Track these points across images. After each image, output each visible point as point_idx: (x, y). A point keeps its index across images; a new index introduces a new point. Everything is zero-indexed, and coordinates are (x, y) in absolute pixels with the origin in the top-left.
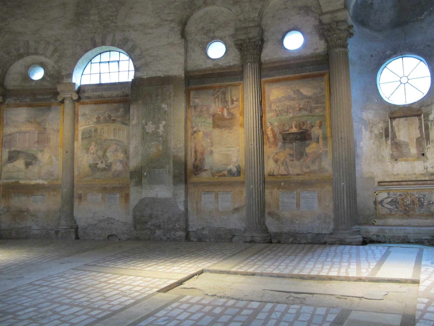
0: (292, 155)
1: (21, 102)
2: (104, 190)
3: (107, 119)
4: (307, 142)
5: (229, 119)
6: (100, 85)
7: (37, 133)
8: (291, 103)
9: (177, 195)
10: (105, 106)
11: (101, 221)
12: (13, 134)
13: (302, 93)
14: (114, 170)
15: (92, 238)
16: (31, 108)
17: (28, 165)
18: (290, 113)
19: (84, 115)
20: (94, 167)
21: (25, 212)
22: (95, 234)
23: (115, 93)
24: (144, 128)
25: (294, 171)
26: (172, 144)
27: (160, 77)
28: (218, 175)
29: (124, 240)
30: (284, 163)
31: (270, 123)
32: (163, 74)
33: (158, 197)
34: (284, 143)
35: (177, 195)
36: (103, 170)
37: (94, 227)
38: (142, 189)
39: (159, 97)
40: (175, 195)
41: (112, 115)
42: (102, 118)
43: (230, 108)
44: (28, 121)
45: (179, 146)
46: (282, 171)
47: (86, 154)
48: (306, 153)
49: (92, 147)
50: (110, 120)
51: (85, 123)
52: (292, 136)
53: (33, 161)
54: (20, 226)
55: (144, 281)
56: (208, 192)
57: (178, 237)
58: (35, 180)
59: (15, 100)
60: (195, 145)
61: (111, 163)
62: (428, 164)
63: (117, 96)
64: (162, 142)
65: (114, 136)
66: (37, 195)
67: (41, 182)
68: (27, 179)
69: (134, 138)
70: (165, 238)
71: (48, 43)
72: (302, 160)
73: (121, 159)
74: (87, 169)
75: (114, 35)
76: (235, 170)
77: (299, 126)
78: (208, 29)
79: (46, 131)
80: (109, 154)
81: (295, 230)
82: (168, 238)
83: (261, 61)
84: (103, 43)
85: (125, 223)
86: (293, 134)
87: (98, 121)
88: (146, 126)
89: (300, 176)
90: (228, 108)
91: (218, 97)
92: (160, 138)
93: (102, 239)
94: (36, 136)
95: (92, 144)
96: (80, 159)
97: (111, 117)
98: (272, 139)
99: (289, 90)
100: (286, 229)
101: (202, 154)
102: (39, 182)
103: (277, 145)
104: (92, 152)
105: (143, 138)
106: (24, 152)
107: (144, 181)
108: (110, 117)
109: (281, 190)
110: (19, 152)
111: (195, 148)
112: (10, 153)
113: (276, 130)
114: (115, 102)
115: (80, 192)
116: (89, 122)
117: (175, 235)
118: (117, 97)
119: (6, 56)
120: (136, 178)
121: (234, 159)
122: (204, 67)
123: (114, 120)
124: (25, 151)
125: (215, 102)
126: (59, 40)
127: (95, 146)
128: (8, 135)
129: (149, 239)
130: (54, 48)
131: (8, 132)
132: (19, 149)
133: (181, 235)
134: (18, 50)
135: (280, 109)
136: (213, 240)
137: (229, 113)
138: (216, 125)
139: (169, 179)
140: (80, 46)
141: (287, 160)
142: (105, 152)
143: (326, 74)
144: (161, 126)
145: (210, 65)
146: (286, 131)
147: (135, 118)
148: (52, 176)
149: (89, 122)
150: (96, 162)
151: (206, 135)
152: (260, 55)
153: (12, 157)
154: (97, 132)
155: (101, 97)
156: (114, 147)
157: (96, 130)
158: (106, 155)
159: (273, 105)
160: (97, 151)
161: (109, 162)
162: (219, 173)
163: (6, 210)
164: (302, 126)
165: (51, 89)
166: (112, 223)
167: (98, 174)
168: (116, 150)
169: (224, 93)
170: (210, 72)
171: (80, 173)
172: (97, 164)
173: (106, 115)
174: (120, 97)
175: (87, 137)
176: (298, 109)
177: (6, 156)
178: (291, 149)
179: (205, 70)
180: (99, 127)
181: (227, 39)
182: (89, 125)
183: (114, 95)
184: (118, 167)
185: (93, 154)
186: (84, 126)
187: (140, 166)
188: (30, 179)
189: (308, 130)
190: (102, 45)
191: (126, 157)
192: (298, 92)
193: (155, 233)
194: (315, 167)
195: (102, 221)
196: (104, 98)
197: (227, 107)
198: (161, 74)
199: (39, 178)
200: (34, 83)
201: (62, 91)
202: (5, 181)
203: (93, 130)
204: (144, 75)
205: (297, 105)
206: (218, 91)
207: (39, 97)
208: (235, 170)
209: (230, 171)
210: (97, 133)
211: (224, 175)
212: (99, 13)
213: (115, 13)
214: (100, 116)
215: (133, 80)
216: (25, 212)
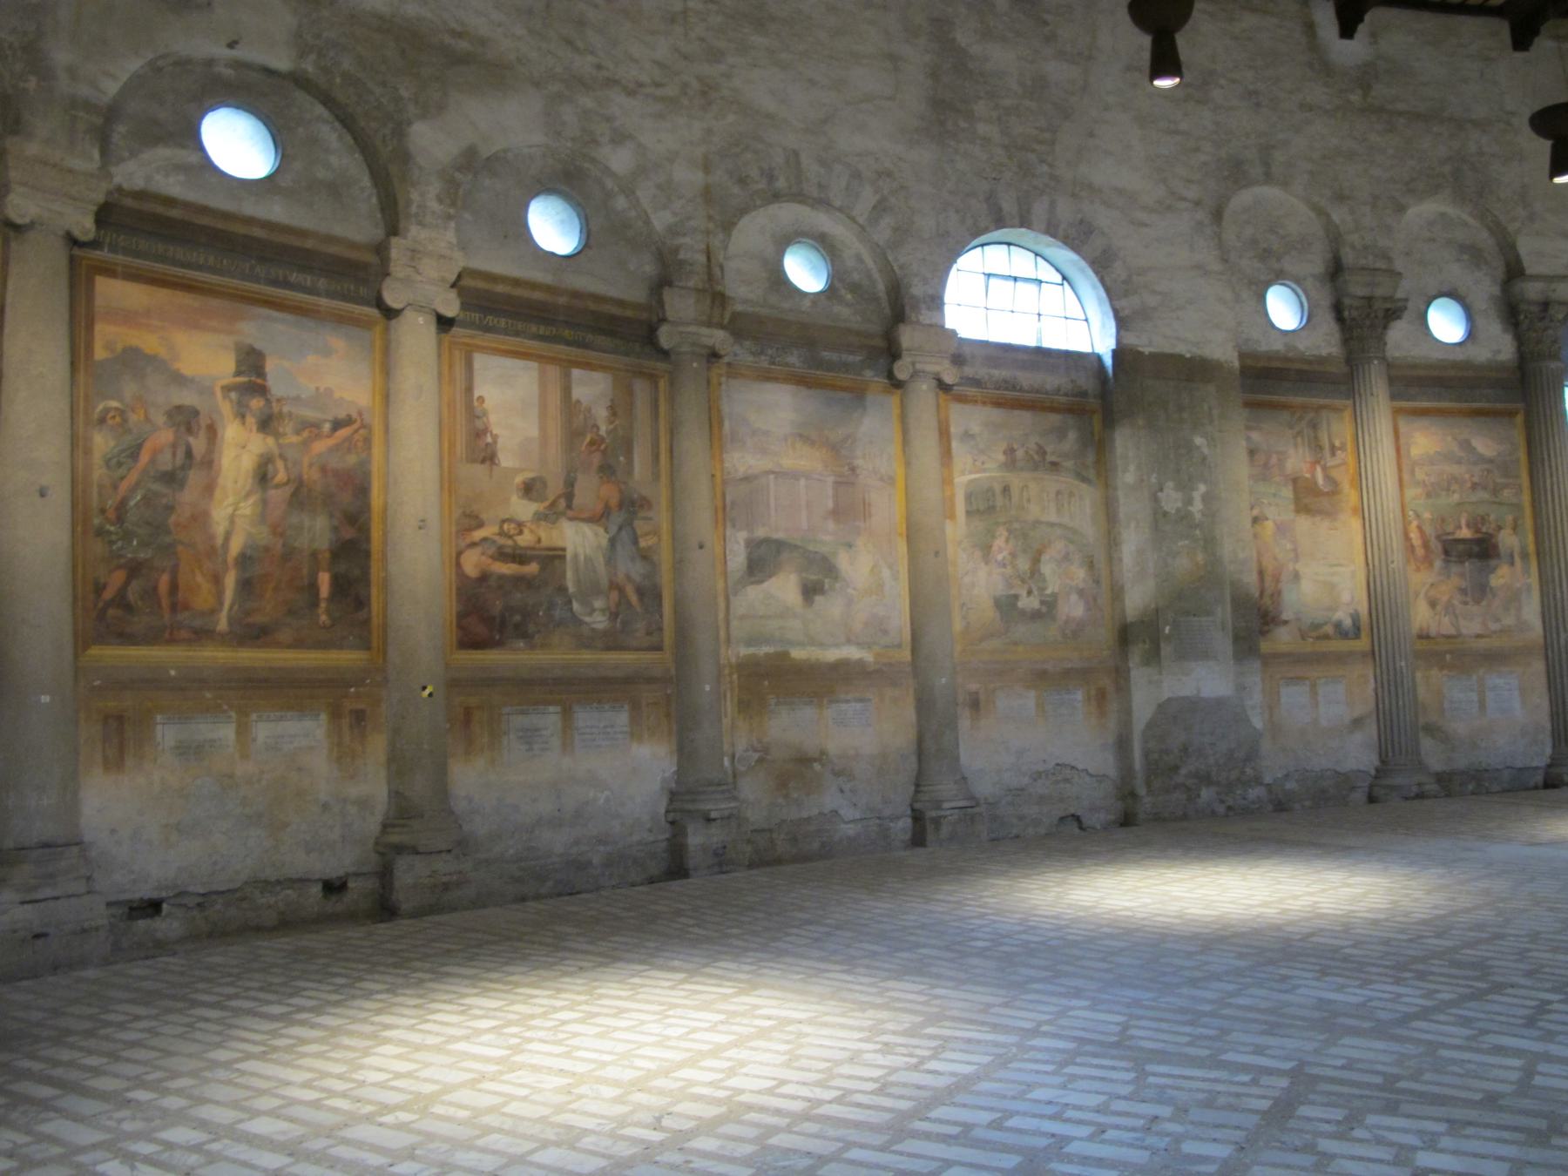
0: (1463, 591)
1: (774, 363)
2: (1041, 678)
3: (1036, 457)
4: (1493, 562)
5: (1327, 493)
6: (1039, 351)
7: (831, 479)
8: (1455, 469)
9: (1245, 688)
10: (1026, 417)
11: (1037, 776)
12: (756, 477)
13: (1475, 449)
14: (1064, 618)
15: (1015, 831)
16: (803, 391)
17: (810, 591)
18: (1454, 492)
19: (967, 436)
20: (1006, 606)
21: (815, 760)
22: (1021, 818)
23: (1052, 381)
24: (1156, 499)
25: (1471, 627)
26: (1227, 549)
27: (1181, 357)
28: (1314, 634)
29: (1099, 827)
30: (1450, 608)
31: (1415, 511)
32: (1189, 352)
33: (1202, 695)
34: (1447, 561)
35: (1245, 688)
36: (1036, 616)
37: (1019, 795)
38: (1160, 673)
39: (1185, 415)
40: (1241, 688)
41: (1049, 449)
42: (1020, 453)
43: (1328, 464)
44: (801, 436)
45: (1241, 556)
46: (1446, 627)
47: (983, 565)
48: (1491, 589)
49: (999, 542)
50: (1042, 463)
51: (974, 464)
52: (1461, 547)
53: (826, 581)
54: (805, 815)
55: (558, 1023)
56: (1297, 680)
57: (1253, 803)
58: (837, 645)
59: (753, 354)
60: (1259, 554)
61: (1055, 596)
63: (1057, 391)
64: (1202, 543)
65: (1059, 511)
66: (847, 701)
67: (853, 653)
68: (813, 642)
69: (1133, 525)
70: (1221, 809)
71: (857, 175)
72: (1484, 603)
73: (1081, 585)
74: (989, 613)
75: (1053, 204)
76: (1348, 622)
77: (1474, 524)
78: (1265, 246)
79: (857, 476)
80: (1047, 569)
81: (1480, 763)
82: (1229, 808)
83: (580, 248)
84: (1024, 222)
85: (1100, 778)
86: (1463, 541)
87: (1011, 463)
88: (1159, 494)
89: (1484, 640)
90: (1325, 465)
91: (1299, 433)
92: (1198, 532)
93: (1042, 831)
94: (830, 492)
95: (998, 533)
96: (967, 580)
97: (1045, 453)
99: (1449, 438)
100: (1461, 762)
101: (1277, 580)
102: (849, 656)
103: (1431, 565)
104: (1000, 557)
105: (1156, 527)
106: (796, 547)
107: (1166, 649)
108: (1042, 452)
109: (1445, 672)
110: (780, 546)
111: (1259, 562)
112: (753, 545)
113: (1428, 530)
114: (1053, 410)
115: (974, 687)
116: (983, 463)
117: (1244, 799)
118: (1057, 394)
119: (736, 190)
120: (1144, 642)
121: (1345, 597)
122: (1263, 348)
123: (1054, 464)
124: (799, 543)
125: (1296, 446)
126: (889, 174)
127: (1007, 541)
128: (741, 479)
129: (1185, 817)
130: (877, 197)
131: (742, 470)
132: (780, 535)
133: (1258, 797)
134: (771, 177)
135: (1433, 480)
136: (1307, 803)
137: (1327, 477)
138: (1302, 508)
139: (1223, 644)
140: (957, 212)
141: (1455, 602)
142: (1036, 560)
143: (1517, 413)
144: (1197, 496)
146: (1449, 534)
147: (1132, 468)
148: (885, 632)
149: (983, 463)
150: (1012, 592)
151: (1281, 529)
153: (762, 561)
154: (1010, 496)
155: (1014, 388)
156: (1058, 547)
157: (1006, 490)
158: (1039, 571)
159: (1417, 469)
160: (1013, 555)
161: (1048, 592)
162: (1313, 631)
163: (756, 756)
164: (1480, 526)
165: (858, 333)
166: (1066, 780)
167: (1021, 630)
168: (1066, 558)
169: (1314, 426)
170: (1278, 364)
171: (968, 623)
172: (1016, 597)
173: (1032, 446)
174: (1066, 395)
175: (982, 508)
176: (1469, 485)
177: (738, 559)
178: (1462, 575)
179: (1270, 356)
180: (1016, 480)
181: (1309, 283)
182: (984, 471)
183: (1048, 387)
184: (1073, 609)
185: (1004, 566)
186: (971, 473)
187: (1153, 606)
188: (822, 645)
189: (1491, 536)
190: (1022, 226)
191: (1094, 581)
192: (1466, 445)
193: (1199, 796)
194: (1509, 621)
195: (1040, 777)
196: (1021, 390)
197: (1322, 463)
198: (1181, 349)
199: (849, 641)
200: (807, 303)
201: (910, 350)
202: (744, 651)
203: (998, 488)
204: (1148, 342)
205: (1467, 476)
206: (1301, 418)
207: (826, 355)
208: (1348, 622)
209: (1338, 625)
210: (1010, 499)
211: (1327, 637)
212: (999, 119)
213: (1047, 136)
214: (1015, 446)
215: (953, 333)
216: (815, 760)
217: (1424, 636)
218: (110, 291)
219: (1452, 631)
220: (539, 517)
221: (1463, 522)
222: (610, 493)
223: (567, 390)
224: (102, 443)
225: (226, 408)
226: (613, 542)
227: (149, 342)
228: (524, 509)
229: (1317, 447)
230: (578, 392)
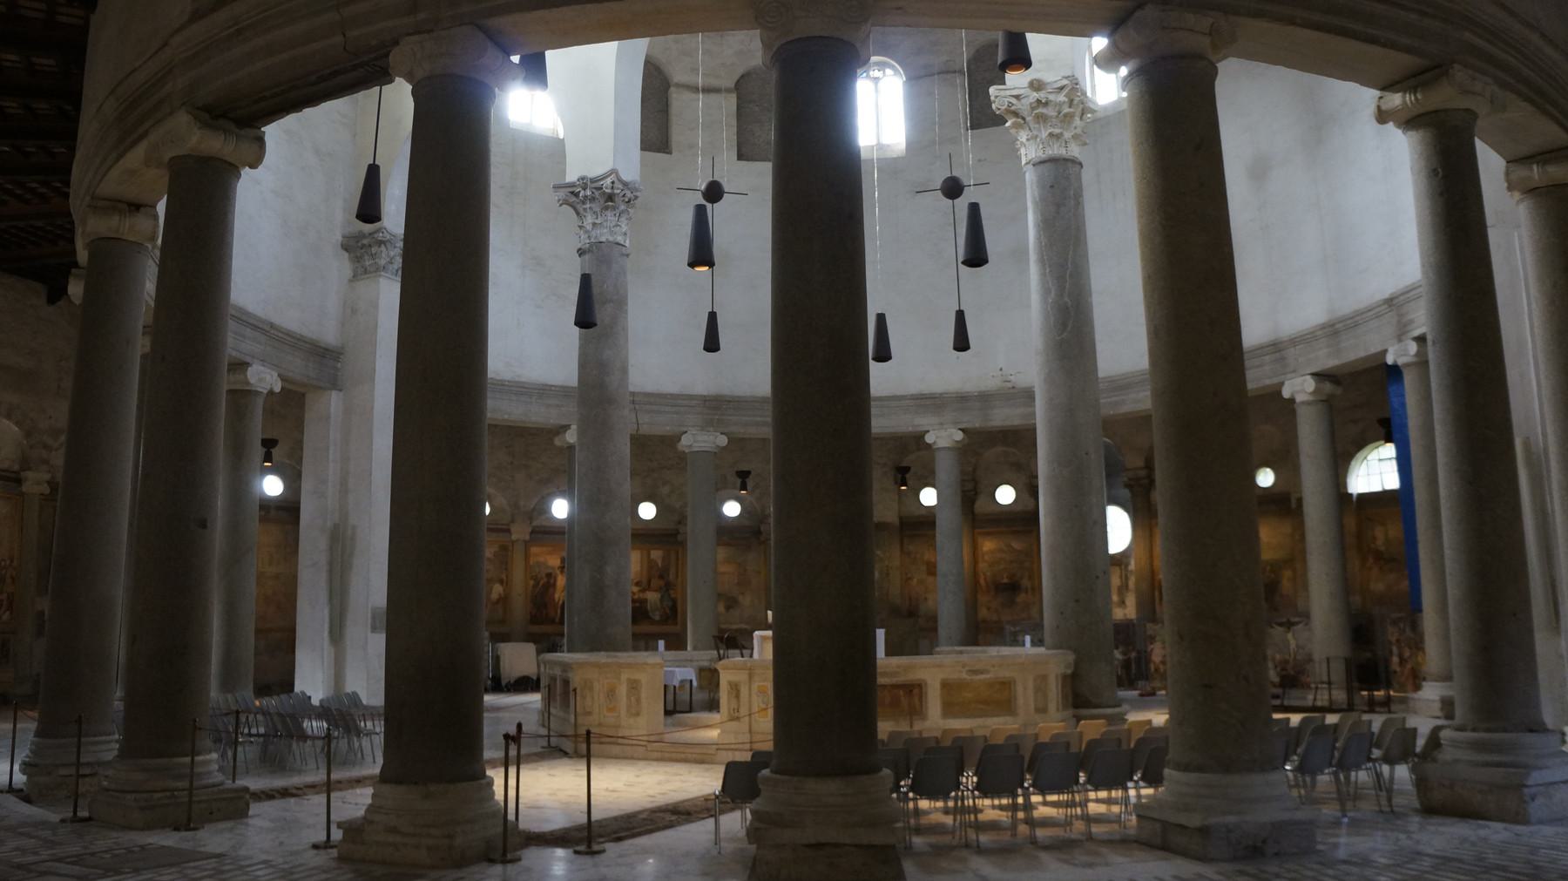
17: (728, 608)
62: (1127, 611)
145: (923, 512)
218: (534, 550)
220: (640, 591)
221: (1005, 576)
222: (662, 583)
223: (649, 554)
224: (532, 582)
225: (558, 572)
226: (662, 597)
227: (541, 559)
228: (635, 589)
230: (652, 557)
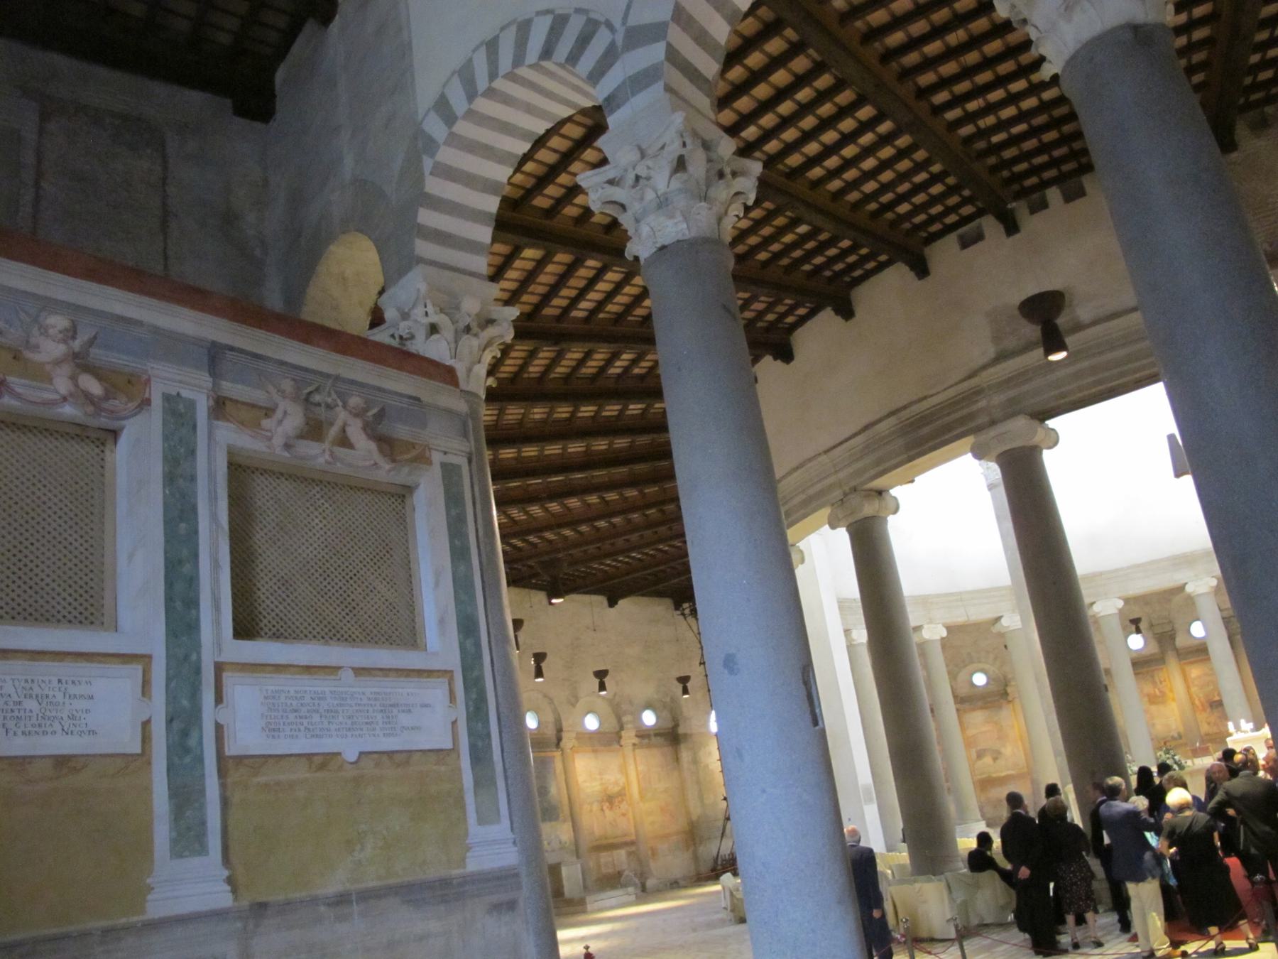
17: (995, 759)
76: (1176, 735)
98: (1201, 708)
110: (985, 750)
113: (1202, 699)
121: (1174, 727)
137: (1161, 692)
152: (1174, 644)
169: (1153, 677)
202: (979, 777)
207: (989, 699)
208: (1176, 735)
217: (1207, 735)
219: (1218, 731)
229: (1154, 683)
